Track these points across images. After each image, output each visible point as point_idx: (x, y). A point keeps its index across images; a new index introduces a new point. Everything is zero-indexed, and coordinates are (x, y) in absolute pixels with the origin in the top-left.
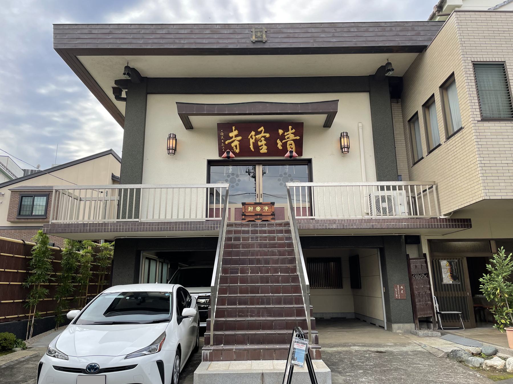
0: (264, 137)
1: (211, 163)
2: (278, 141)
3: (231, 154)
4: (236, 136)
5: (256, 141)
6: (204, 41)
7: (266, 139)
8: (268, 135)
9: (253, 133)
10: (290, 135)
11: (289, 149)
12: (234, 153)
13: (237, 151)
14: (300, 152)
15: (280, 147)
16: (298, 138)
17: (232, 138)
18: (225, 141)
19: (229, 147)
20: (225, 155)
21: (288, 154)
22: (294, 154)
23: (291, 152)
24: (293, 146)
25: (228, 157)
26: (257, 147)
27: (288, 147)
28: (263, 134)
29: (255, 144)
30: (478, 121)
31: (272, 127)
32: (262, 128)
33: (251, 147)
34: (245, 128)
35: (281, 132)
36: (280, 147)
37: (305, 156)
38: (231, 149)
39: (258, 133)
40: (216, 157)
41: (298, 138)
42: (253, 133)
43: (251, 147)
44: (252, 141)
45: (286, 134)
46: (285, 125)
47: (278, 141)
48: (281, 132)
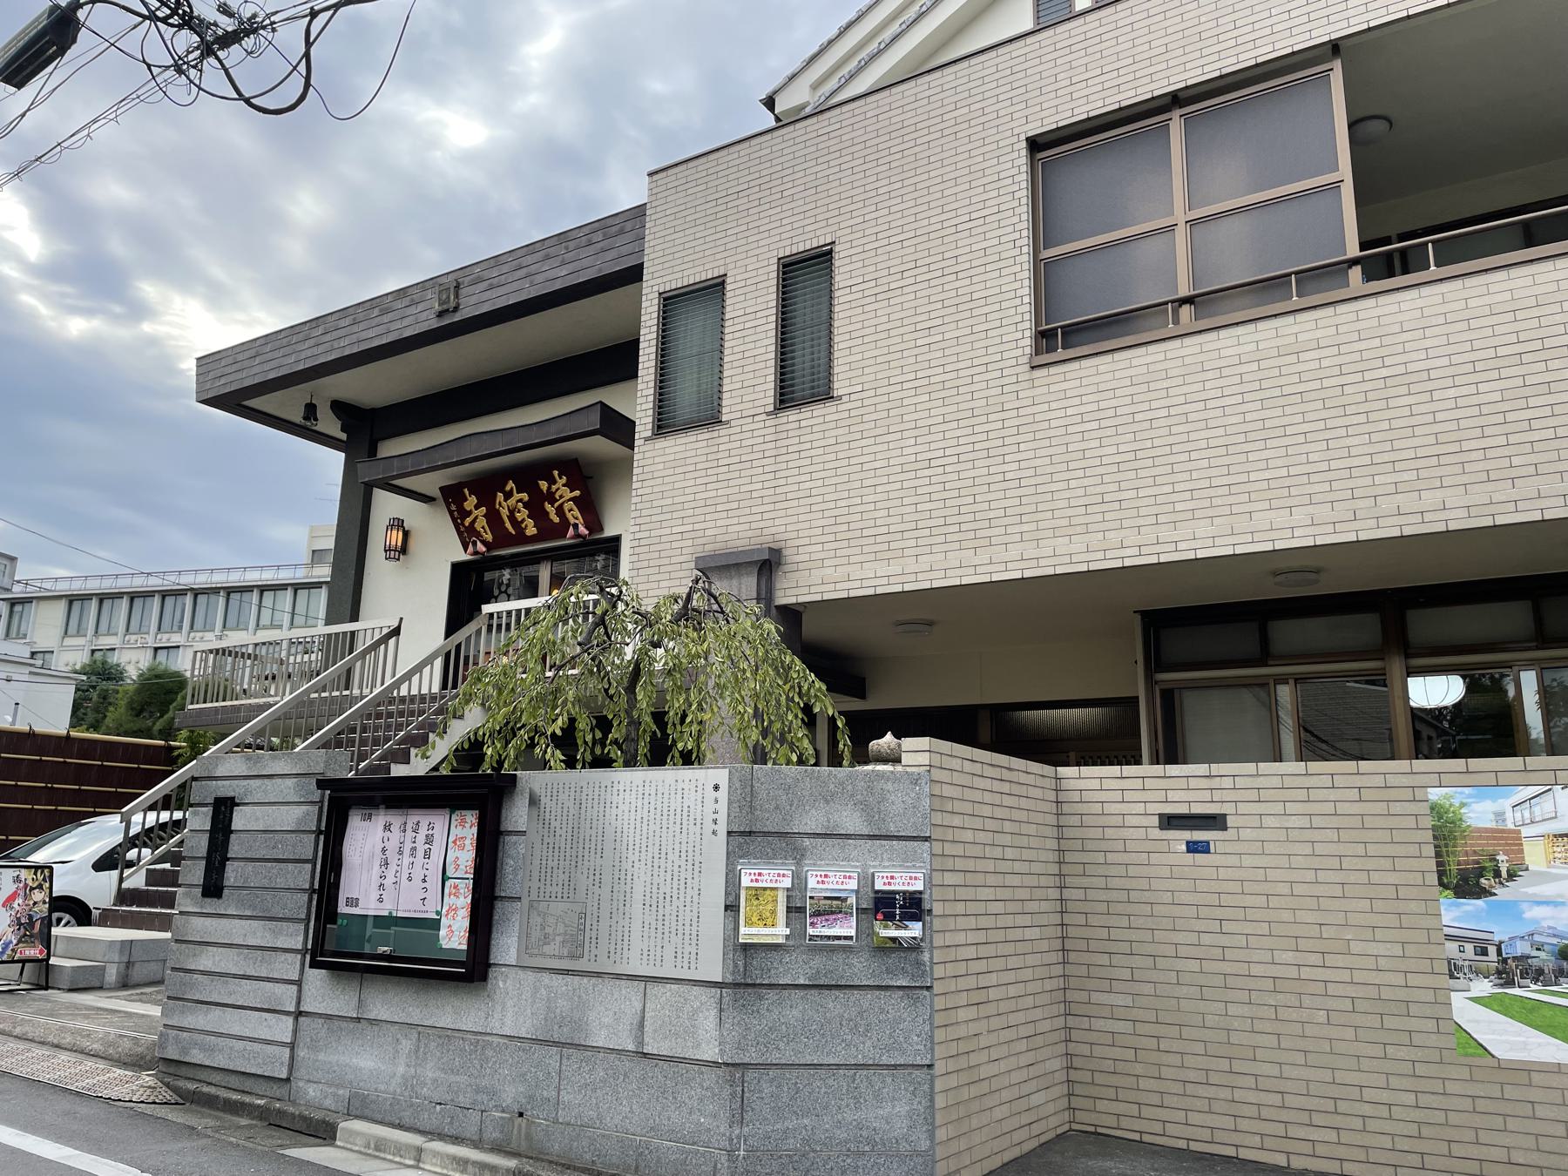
0: (520, 500)
1: (456, 567)
2: (548, 506)
3: (481, 547)
4: (477, 507)
5: (512, 512)
6: (371, 333)
7: (526, 505)
8: (525, 496)
9: (500, 496)
10: (564, 492)
11: (572, 521)
12: (484, 542)
13: (489, 537)
14: (595, 524)
15: (556, 520)
16: (577, 493)
17: (470, 513)
18: (463, 519)
19: (472, 530)
20: (471, 548)
21: (571, 531)
22: (583, 530)
23: (576, 526)
24: (577, 513)
25: (476, 553)
26: (516, 523)
27: (569, 515)
28: (517, 496)
29: (512, 518)
30: (768, 414)
31: (527, 476)
32: (511, 485)
33: (508, 525)
34: (486, 487)
35: (544, 485)
36: (556, 520)
37: (609, 532)
38: (478, 535)
39: (508, 495)
40: (462, 556)
41: (577, 493)
42: (500, 496)
43: (508, 525)
44: (505, 513)
45: (554, 487)
46: (543, 469)
47: (548, 506)
48: (544, 485)
